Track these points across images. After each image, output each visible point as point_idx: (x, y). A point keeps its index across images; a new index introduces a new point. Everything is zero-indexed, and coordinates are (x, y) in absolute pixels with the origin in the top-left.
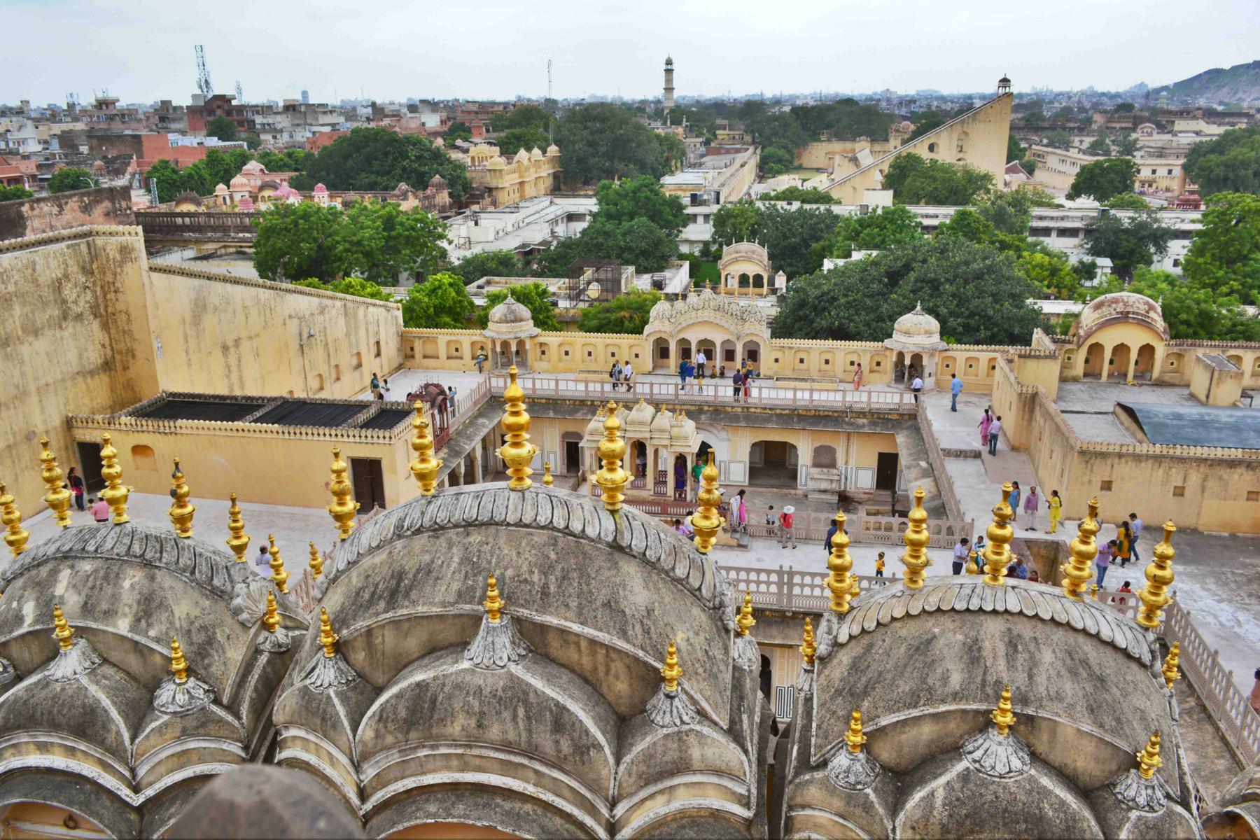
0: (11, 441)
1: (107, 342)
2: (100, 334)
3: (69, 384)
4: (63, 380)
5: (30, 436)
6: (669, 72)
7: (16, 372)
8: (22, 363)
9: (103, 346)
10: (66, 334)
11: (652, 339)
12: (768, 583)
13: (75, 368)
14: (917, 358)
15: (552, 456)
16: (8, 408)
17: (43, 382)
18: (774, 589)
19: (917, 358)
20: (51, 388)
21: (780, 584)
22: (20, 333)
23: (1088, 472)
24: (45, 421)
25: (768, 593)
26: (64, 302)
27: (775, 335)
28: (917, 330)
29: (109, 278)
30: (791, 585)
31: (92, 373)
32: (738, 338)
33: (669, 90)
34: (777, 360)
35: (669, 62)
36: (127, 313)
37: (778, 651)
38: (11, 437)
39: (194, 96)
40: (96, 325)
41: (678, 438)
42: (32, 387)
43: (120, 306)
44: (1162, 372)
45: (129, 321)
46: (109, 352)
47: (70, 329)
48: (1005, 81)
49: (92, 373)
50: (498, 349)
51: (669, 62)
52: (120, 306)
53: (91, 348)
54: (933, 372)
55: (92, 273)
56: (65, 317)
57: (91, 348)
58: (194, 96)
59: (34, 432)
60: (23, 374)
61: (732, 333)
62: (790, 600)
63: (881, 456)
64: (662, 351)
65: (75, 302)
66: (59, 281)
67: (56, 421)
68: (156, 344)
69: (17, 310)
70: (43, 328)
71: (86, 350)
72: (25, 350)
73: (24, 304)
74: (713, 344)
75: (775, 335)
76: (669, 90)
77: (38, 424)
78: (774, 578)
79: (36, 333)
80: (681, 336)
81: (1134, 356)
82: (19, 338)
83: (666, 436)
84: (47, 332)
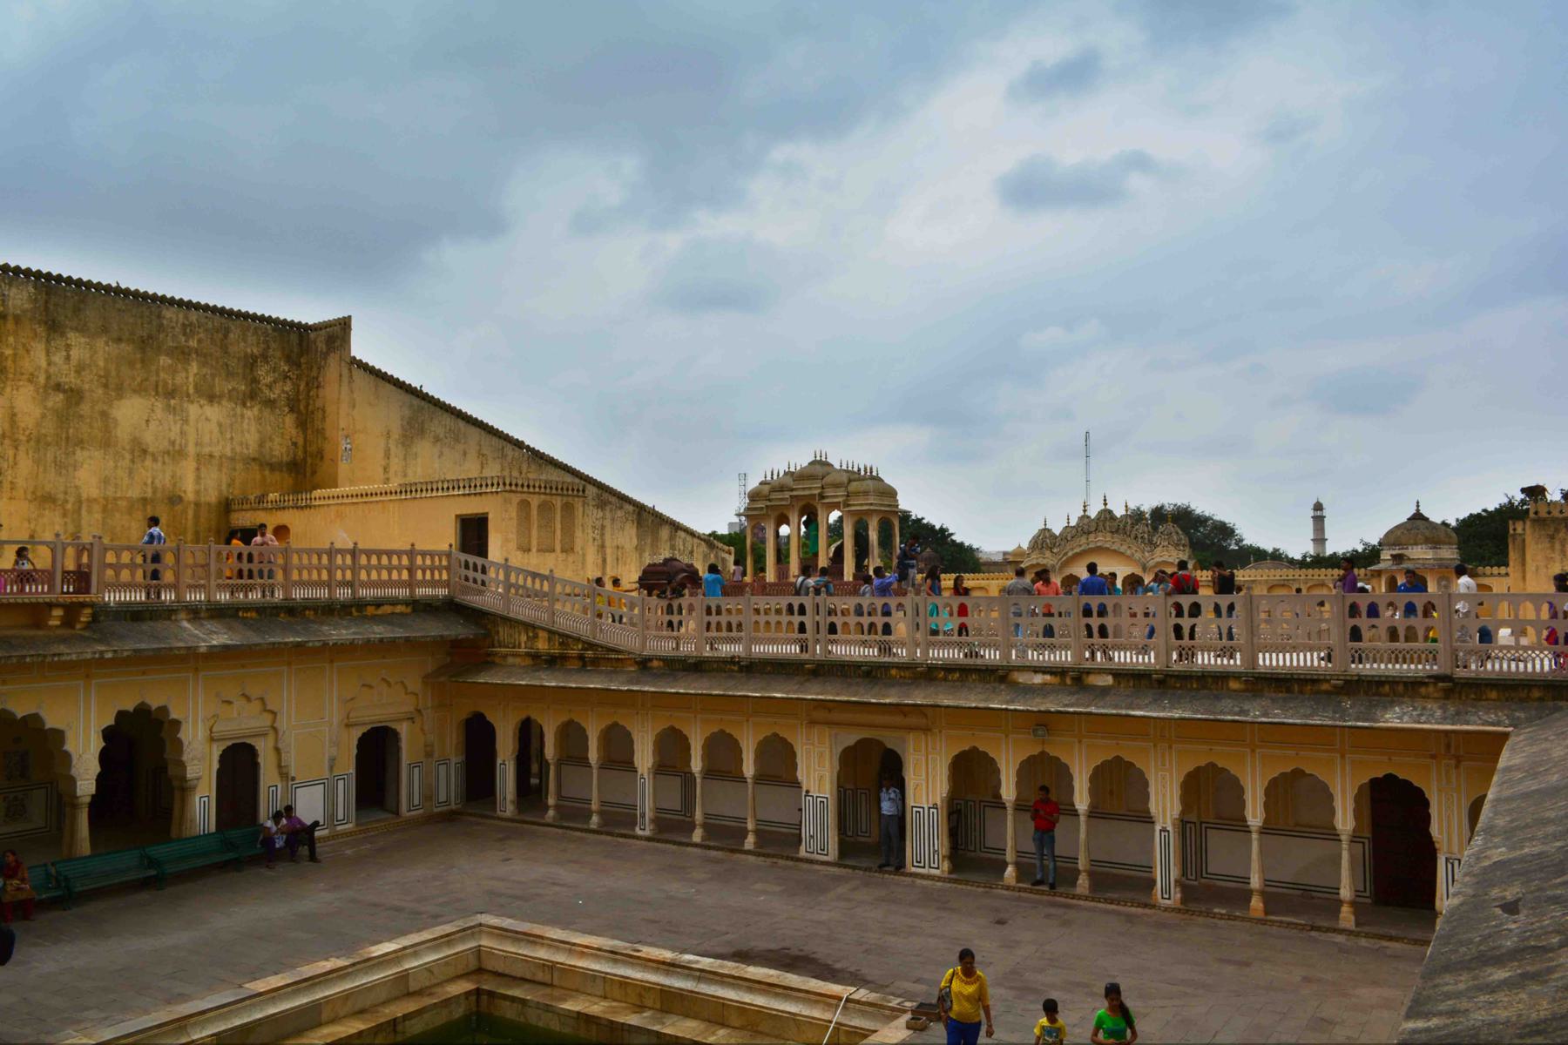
0: (149, 495)
1: (301, 442)
2: (294, 432)
3: (240, 466)
4: (232, 459)
5: (174, 500)
6: (1319, 521)
7: (176, 429)
8: (186, 421)
9: (295, 444)
10: (248, 413)
13: (252, 450)
16: (155, 460)
17: (207, 450)
20: (215, 462)
22: (191, 391)
23: (1557, 556)
24: (197, 492)
26: (255, 381)
29: (314, 373)
31: (273, 467)
32: (1144, 569)
33: (1320, 540)
35: (1318, 507)
36: (324, 411)
37: (911, 738)
38: (149, 490)
39: (731, 525)
40: (289, 420)
41: (857, 494)
42: (191, 449)
43: (319, 403)
45: (324, 418)
46: (300, 453)
47: (256, 410)
49: (273, 467)
51: (1318, 507)
52: (319, 403)
53: (277, 440)
55: (299, 365)
56: (253, 395)
57: (277, 440)
58: (731, 525)
59: (180, 498)
60: (183, 433)
61: (1137, 562)
65: (270, 387)
66: (254, 358)
67: (212, 497)
68: (343, 445)
69: (194, 367)
70: (221, 397)
71: (271, 440)
72: (193, 410)
73: (203, 364)
76: (1320, 540)
77: (189, 488)
79: (212, 399)
80: (1067, 572)
82: (188, 396)
83: (841, 492)
84: (224, 402)
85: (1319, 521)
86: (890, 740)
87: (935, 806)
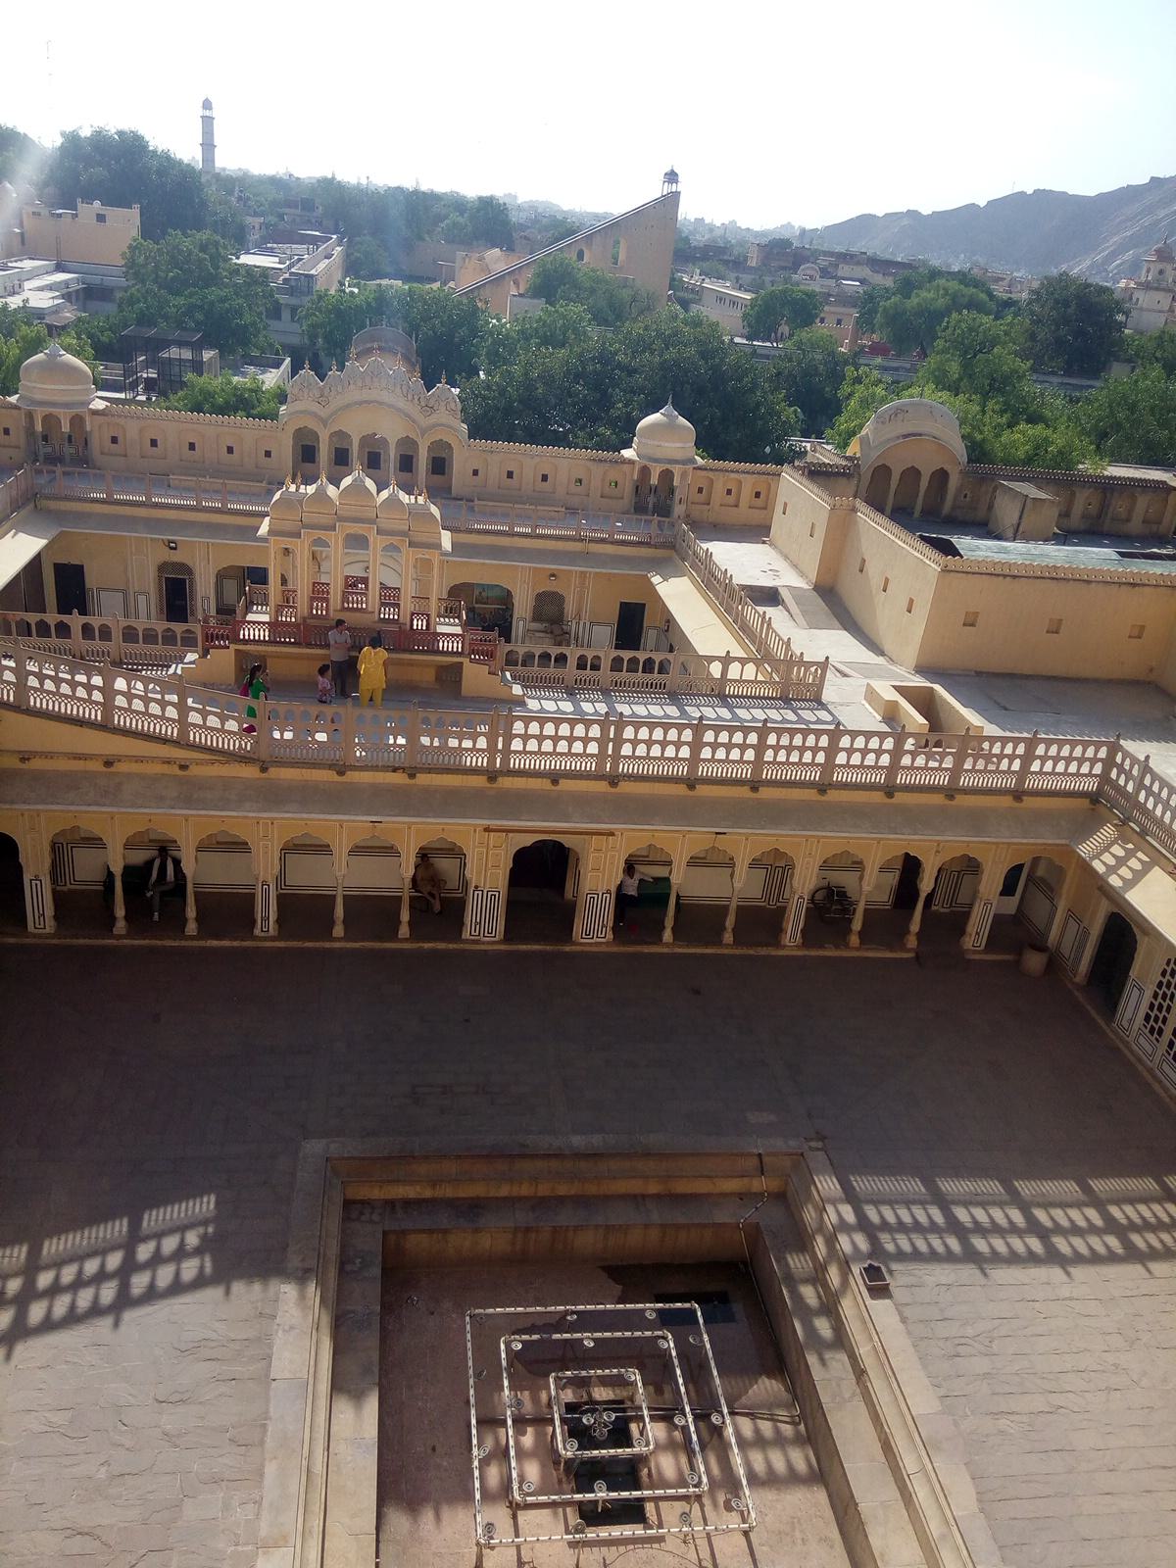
6: (208, 123)
11: (291, 430)
12: (586, 740)
14: (667, 475)
15: (142, 599)
18: (593, 748)
19: (667, 475)
21: (602, 742)
25: (585, 755)
27: (474, 434)
28: (663, 435)
30: (619, 741)
33: (208, 146)
34: (475, 473)
35: (207, 105)
44: (954, 508)
48: (672, 177)
50: (39, 428)
51: (207, 105)
54: (684, 497)
62: (615, 765)
63: (621, 603)
64: (307, 453)
74: (384, 441)
75: (474, 434)
76: (208, 146)
78: (595, 731)
81: (924, 483)
85: (208, 123)
86: (567, 841)
87: (609, 892)
